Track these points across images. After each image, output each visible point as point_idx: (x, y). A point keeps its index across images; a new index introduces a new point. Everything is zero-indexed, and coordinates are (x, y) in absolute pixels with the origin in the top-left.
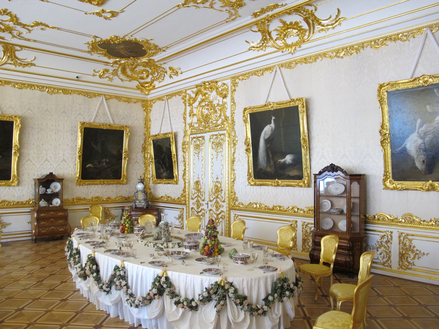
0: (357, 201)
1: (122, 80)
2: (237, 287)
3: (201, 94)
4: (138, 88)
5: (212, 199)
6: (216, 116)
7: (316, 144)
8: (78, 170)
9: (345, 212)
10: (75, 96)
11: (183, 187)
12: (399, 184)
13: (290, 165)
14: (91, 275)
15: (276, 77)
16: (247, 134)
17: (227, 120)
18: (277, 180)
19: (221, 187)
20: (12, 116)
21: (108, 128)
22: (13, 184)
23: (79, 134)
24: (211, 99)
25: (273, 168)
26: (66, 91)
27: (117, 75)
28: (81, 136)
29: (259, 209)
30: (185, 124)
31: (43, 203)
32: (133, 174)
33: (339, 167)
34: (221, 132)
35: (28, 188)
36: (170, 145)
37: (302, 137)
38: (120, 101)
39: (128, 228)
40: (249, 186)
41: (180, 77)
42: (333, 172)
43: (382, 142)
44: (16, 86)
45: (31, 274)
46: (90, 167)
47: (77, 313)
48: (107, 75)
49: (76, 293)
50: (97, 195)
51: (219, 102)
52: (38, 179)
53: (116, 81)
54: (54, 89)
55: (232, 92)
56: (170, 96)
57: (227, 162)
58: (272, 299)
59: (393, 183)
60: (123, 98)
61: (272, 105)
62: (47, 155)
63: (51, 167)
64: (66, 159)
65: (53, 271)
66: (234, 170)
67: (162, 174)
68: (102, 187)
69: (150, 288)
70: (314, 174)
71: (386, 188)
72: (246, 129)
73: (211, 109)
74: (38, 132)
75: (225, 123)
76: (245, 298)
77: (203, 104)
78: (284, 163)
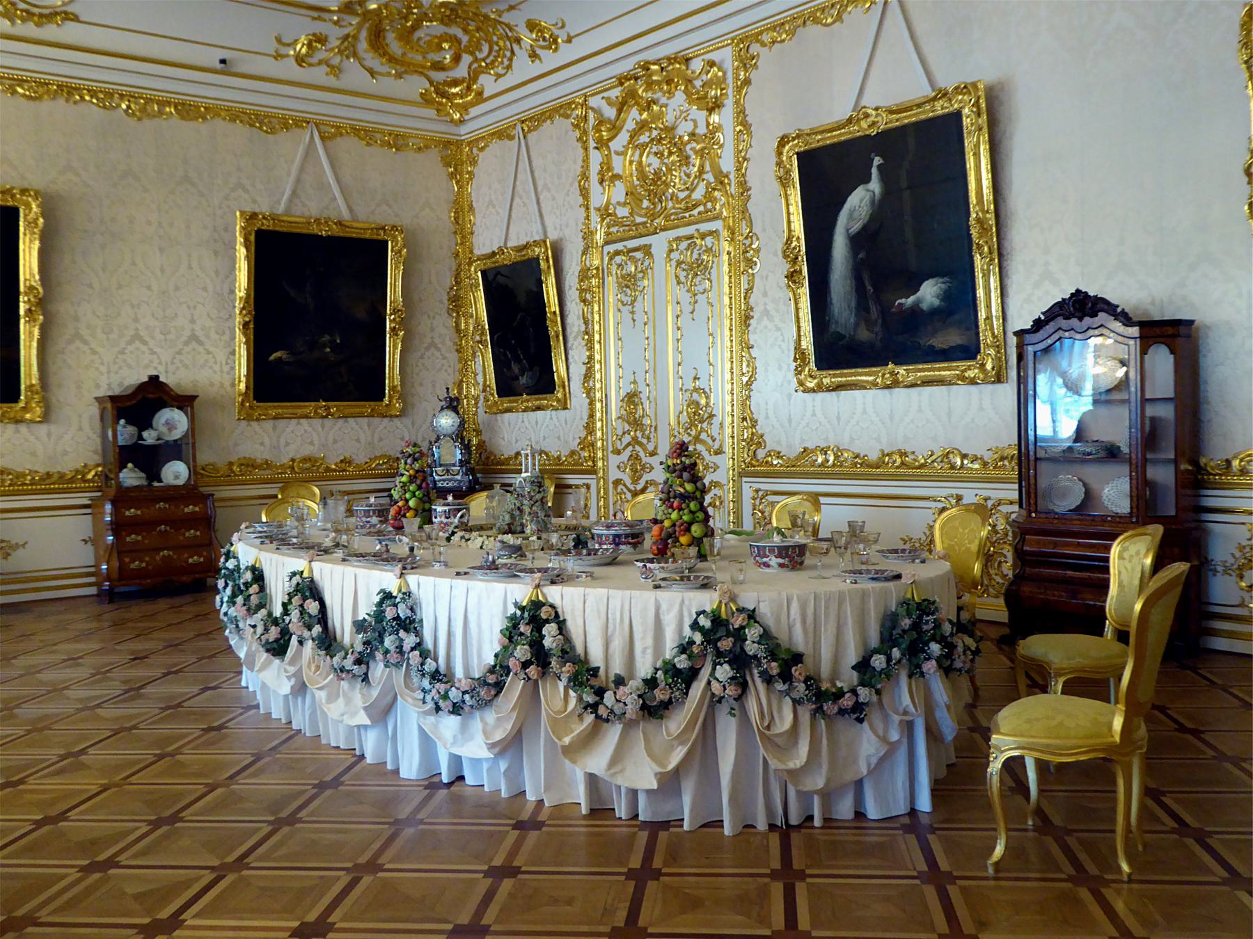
0: (1166, 412)
1: (372, 73)
2: (770, 622)
3: (637, 103)
4: (426, 100)
6: (688, 176)
7: (1020, 236)
8: (244, 371)
9: (1125, 450)
10: (220, 125)
11: (585, 416)
13: (934, 312)
14: (306, 634)
15: (887, 23)
16: (789, 222)
17: (722, 183)
18: (891, 366)
19: (707, 404)
20: (13, 188)
21: (336, 231)
22: (28, 416)
23: (241, 252)
24: (670, 118)
25: (878, 329)
26: (187, 110)
27: (355, 55)
28: (247, 257)
29: (834, 465)
30: (588, 209)
31: (131, 477)
32: (421, 385)
33: (1103, 300)
34: (704, 227)
35: (80, 429)
36: (540, 282)
37: (974, 215)
38: (368, 144)
39: (416, 510)
41: (567, 53)
42: (1081, 319)
44: (20, 90)
45: (101, 675)
46: (280, 358)
47: (258, 758)
48: (321, 55)
49: (253, 711)
50: (307, 451)
51: (696, 126)
52: (113, 399)
53: (354, 75)
54: (149, 101)
55: (739, 90)
56: (535, 120)
57: (727, 322)
58: (884, 665)
60: (378, 136)
62: (136, 320)
64: (199, 333)
65: (176, 665)
66: (750, 347)
67: (517, 378)
68: (323, 426)
69: (498, 648)
70: (1016, 334)
72: (788, 205)
73: (671, 153)
74: (103, 247)
75: (716, 193)
76: (797, 658)
77: (644, 138)
78: (915, 311)
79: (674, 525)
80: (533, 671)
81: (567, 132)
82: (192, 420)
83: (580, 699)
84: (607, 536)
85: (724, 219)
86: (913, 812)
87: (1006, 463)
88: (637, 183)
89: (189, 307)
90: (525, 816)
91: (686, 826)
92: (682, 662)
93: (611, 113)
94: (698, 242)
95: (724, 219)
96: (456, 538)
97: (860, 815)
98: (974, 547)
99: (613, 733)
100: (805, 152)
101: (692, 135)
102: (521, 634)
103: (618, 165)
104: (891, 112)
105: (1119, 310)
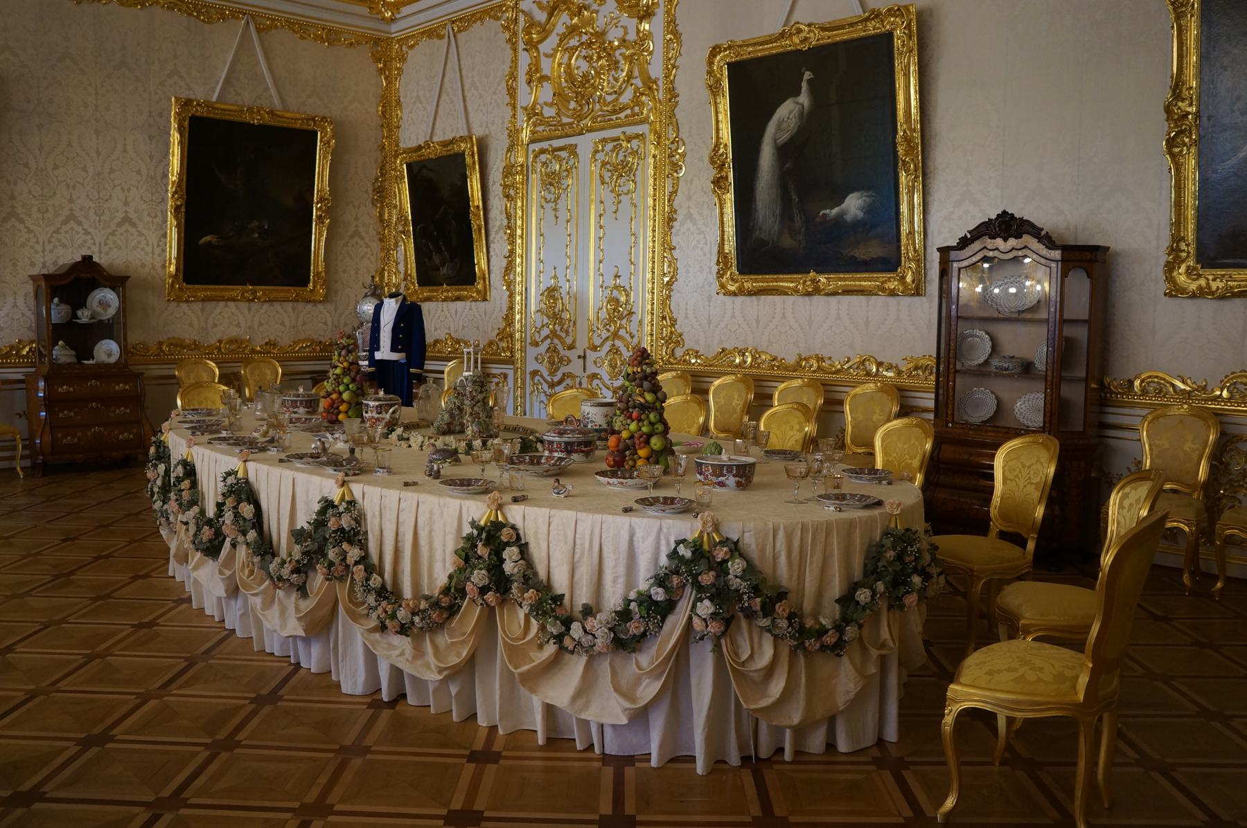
0: (1081, 333)
3: (568, 9)
5: (597, 342)
7: (944, 156)
8: (174, 253)
9: (1040, 365)
12: (1216, 280)
13: (857, 224)
14: (240, 539)
16: (718, 130)
17: (650, 88)
18: (812, 274)
21: (267, 120)
23: (175, 137)
24: (600, 23)
28: (181, 142)
29: (751, 366)
31: (62, 353)
33: (1027, 221)
34: (631, 130)
35: (15, 306)
36: (464, 178)
39: (349, 403)
40: (721, 295)
42: (1005, 240)
43: (1171, 143)
49: (184, 606)
50: (234, 332)
51: (626, 33)
52: (47, 277)
57: (650, 223)
58: (869, 600)
59: (1199, 276)
60: (312, 30)
61: (803, 35)
62: (71, 201)
63: (85, 241)
64: (133, 215)
66: (672, 249)
68: (249, 309)
70: (939, 249)
71: (1175, 291)
72: (717, 113)
73: (600, 58)
75: (644, 98)
77: (574, 42)
79: (632, 437)
80: (490, 597)
81: (496, 34)
82: (123, 299)
83: (543, 628)
84: (559, 443)
85: (651, 124)
86: (881, 742)
87: (920, 372)
88: (564, 84)
89: (123, 189)
90: (479, 745)
91: (654, 763)
92: (659, 594)
93: (541, 16)
94: (624, 144)
95: (651, 124)
96: (394, 436)
97: (831, 746)
98: (916, 463)
99: (576, 666)
100: (736, 63)
101: (623, 41)
102: (480, 557)
103: (546, 66)
104: (823, 29)
105: (1043, 233)
